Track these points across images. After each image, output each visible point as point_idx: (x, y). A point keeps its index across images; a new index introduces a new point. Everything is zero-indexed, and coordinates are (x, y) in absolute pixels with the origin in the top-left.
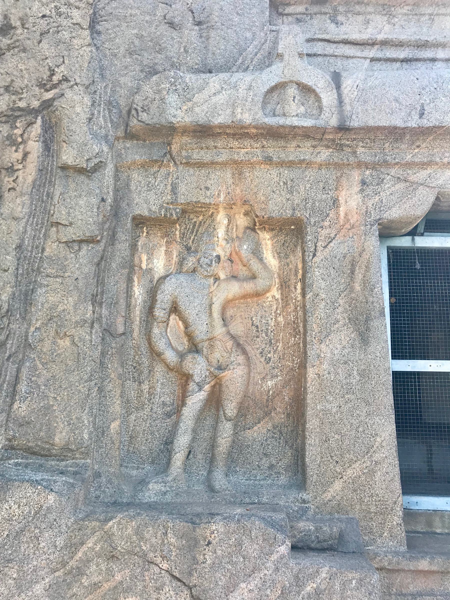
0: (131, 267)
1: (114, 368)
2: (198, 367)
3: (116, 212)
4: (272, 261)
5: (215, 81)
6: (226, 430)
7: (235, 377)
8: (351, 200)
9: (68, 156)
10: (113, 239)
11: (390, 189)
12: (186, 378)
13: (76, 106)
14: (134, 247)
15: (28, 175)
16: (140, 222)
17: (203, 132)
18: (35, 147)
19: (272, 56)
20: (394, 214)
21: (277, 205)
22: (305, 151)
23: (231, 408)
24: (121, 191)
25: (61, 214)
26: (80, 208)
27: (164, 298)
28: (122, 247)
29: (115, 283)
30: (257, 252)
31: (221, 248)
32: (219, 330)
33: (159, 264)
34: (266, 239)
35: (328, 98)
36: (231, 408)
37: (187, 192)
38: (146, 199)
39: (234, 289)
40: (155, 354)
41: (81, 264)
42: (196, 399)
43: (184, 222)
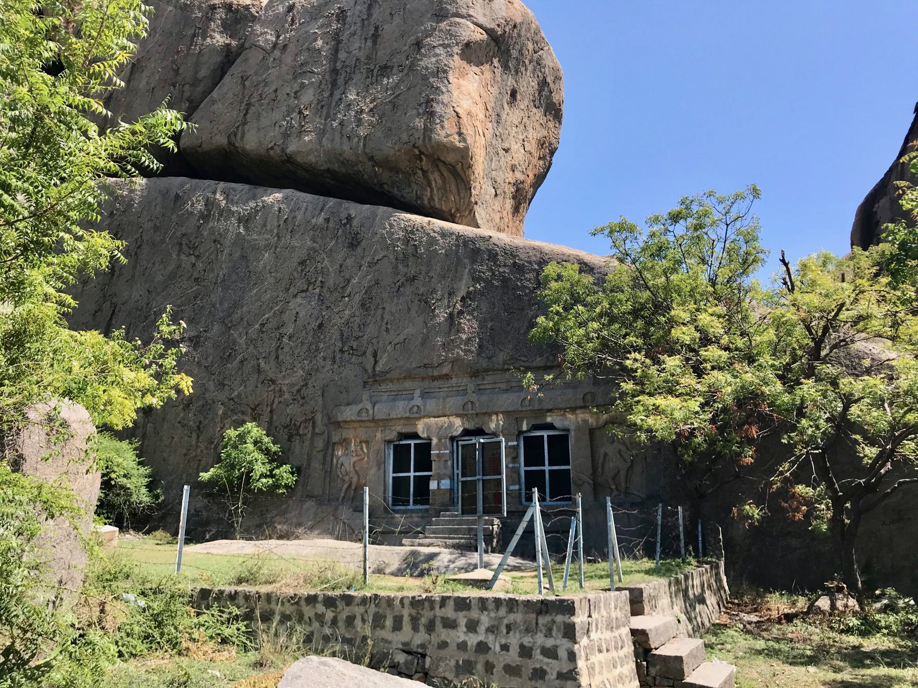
0: (333, 455)
1: (328, 479)
2: (347, 478)
3: (328, 442)
4: (365, 451)
5: (348, 408)
6: (352, 492)
7: (355, 480)
8: (379, 435)
9: (317, 431)
10: (327, 449)
11: (387, 431)
12: (344, 481)
13: (319, 417)
14: (333, 450)
15: (309, 435)
16: (334, 444)
17: (346, 422)
18: (310, 428)
19: (361, 401)
20: (388, 438)
21: (364, 437)
22: (368, 424)
23: (353, 487)
24: (329, 437)
25: (316, 445)
26: (320, 444)
27: (340, 462)
28: (330, 450)
29: (328, 459)
30: (362, 449)
31: (353, 447)
32: (352, 469)
33: (340, 453)
34: (364, 445)
35: (371, 412)
36: (353, 487)
37: (344, 435)
38: (335, 439)
39: (356, 459)
40: (338, 476)
41: (320, 456)
42: (346, 486)
43: (345, 442)
